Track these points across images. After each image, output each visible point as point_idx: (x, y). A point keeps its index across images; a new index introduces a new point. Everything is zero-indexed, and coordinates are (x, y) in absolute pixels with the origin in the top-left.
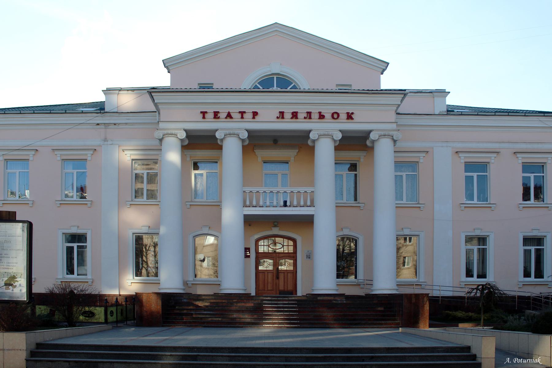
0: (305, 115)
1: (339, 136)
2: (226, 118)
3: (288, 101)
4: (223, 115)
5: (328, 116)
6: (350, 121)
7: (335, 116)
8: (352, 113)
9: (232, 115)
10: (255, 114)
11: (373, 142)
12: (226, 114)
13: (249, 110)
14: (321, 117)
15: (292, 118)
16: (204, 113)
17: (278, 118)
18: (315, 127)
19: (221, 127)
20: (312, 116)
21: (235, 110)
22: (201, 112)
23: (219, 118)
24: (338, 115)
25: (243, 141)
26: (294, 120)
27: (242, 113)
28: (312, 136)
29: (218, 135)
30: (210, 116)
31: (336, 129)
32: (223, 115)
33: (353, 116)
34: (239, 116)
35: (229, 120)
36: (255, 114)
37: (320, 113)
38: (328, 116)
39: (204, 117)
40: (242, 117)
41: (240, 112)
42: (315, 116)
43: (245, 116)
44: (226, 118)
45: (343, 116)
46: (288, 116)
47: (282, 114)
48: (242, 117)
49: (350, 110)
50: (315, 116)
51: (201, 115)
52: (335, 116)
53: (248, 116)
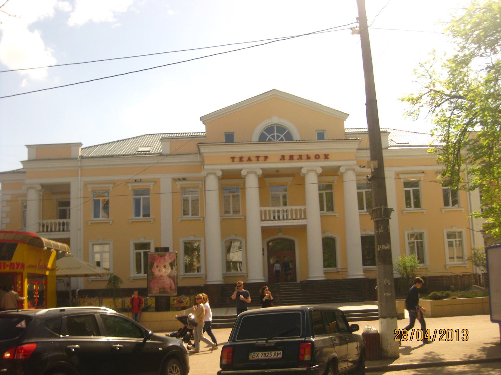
0: (298, 157)
1: (320, 171)
2: (248, 161)
3: (287, 148)
4: (245, 159)
5: (312, 157)
6: (327, 159)
7: (317, 157)
8: (328, 155)
9: (252, 159)
10: (266, 158)
11: (342, 173)
12: (246, 159)
13: (262, 154)
14: (308, 158)
15: (290, 159)
16: (233, 158)
17: (281, 160)
18: (305, 165)
19: (245, 167)
20: (303, 157)
21: (253, 155)
22: (231, 158)
23: (243, 161)
24: (319, 156)
25: (258, 176)
26: (291, 161)
27: (258, 158)
28: (303, 171)
29: (243, 173)
30: (237, 160)
31: (318, 165)
32: (245, 159)
33: (329, 157)
34: (256, 159)
35: (249, 162)
36: (266, 158)
37: (307, 155)
38: (312, 157)
39: (233, 161)
40: (258, 160)
41: (256, 157)
42: (304, 157)
43: (260, 159)
44: (248, 161)
45: (322, 157)
46: (287, 158)
47: (283, 158)
48: (258, 160)
49: (326, 152)
50: (304, 157)
51: (231, 160)
52: (317, 157)
53: (261, 159)
